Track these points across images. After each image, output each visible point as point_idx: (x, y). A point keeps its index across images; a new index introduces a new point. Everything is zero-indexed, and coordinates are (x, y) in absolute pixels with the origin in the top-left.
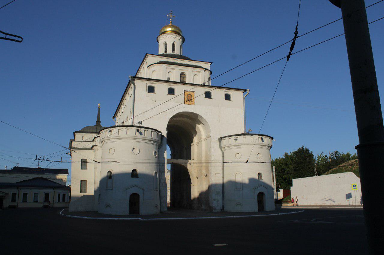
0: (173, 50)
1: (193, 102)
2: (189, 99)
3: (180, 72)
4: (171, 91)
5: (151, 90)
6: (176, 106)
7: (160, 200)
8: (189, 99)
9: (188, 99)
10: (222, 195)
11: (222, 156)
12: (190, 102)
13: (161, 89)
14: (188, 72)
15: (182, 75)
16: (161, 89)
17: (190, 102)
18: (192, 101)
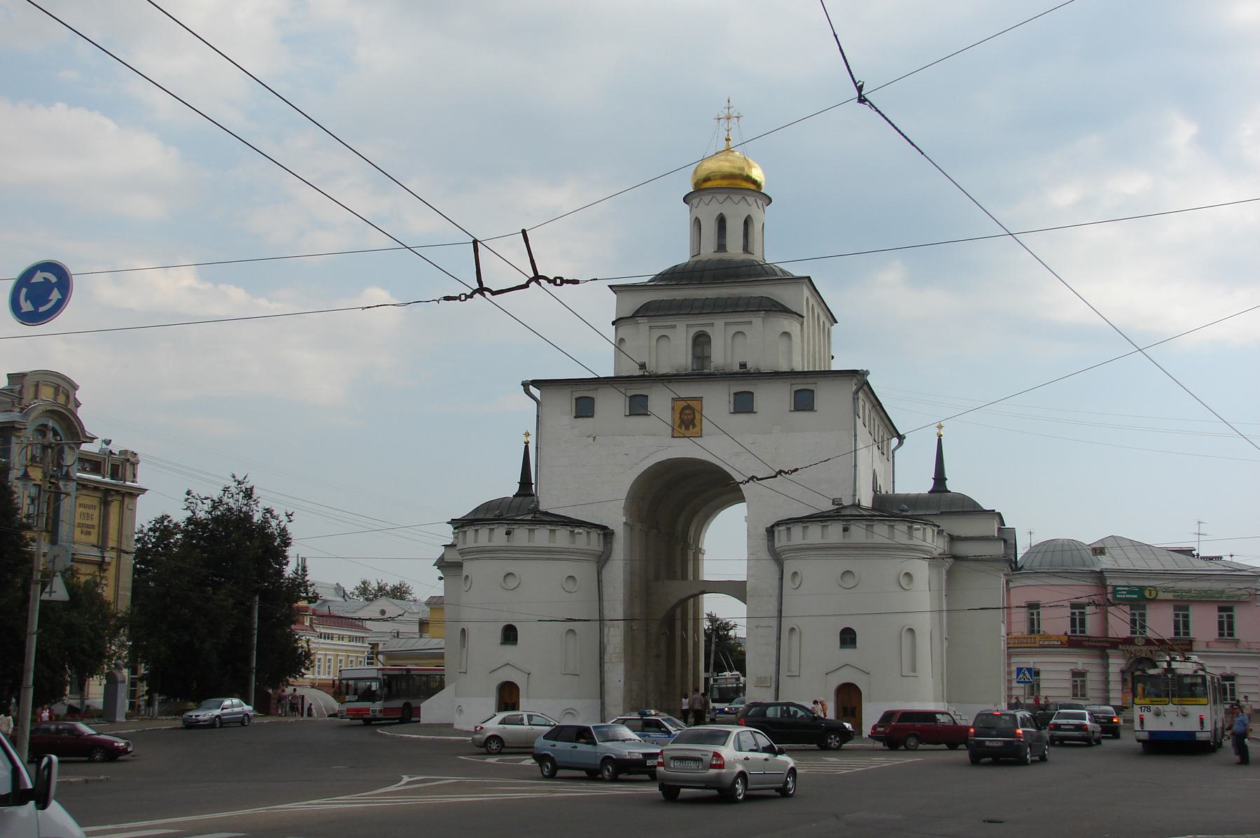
0: (721, 247)
1: (698, 428)
2: (687, 420)
3: (693, 331)
4: (638, 407)
5: (584, 409)
6: (652, 443)
7: (602, 697)
8: (687, 420)
9: (682, 421)
10: (773, 686)
11: (777, 577)
12: (687, 428)
13: (611, 405)
14: (719, 331)
15: (701, 341)
16: (611, 405)
17: (687, 428)
18: (694, 426)
